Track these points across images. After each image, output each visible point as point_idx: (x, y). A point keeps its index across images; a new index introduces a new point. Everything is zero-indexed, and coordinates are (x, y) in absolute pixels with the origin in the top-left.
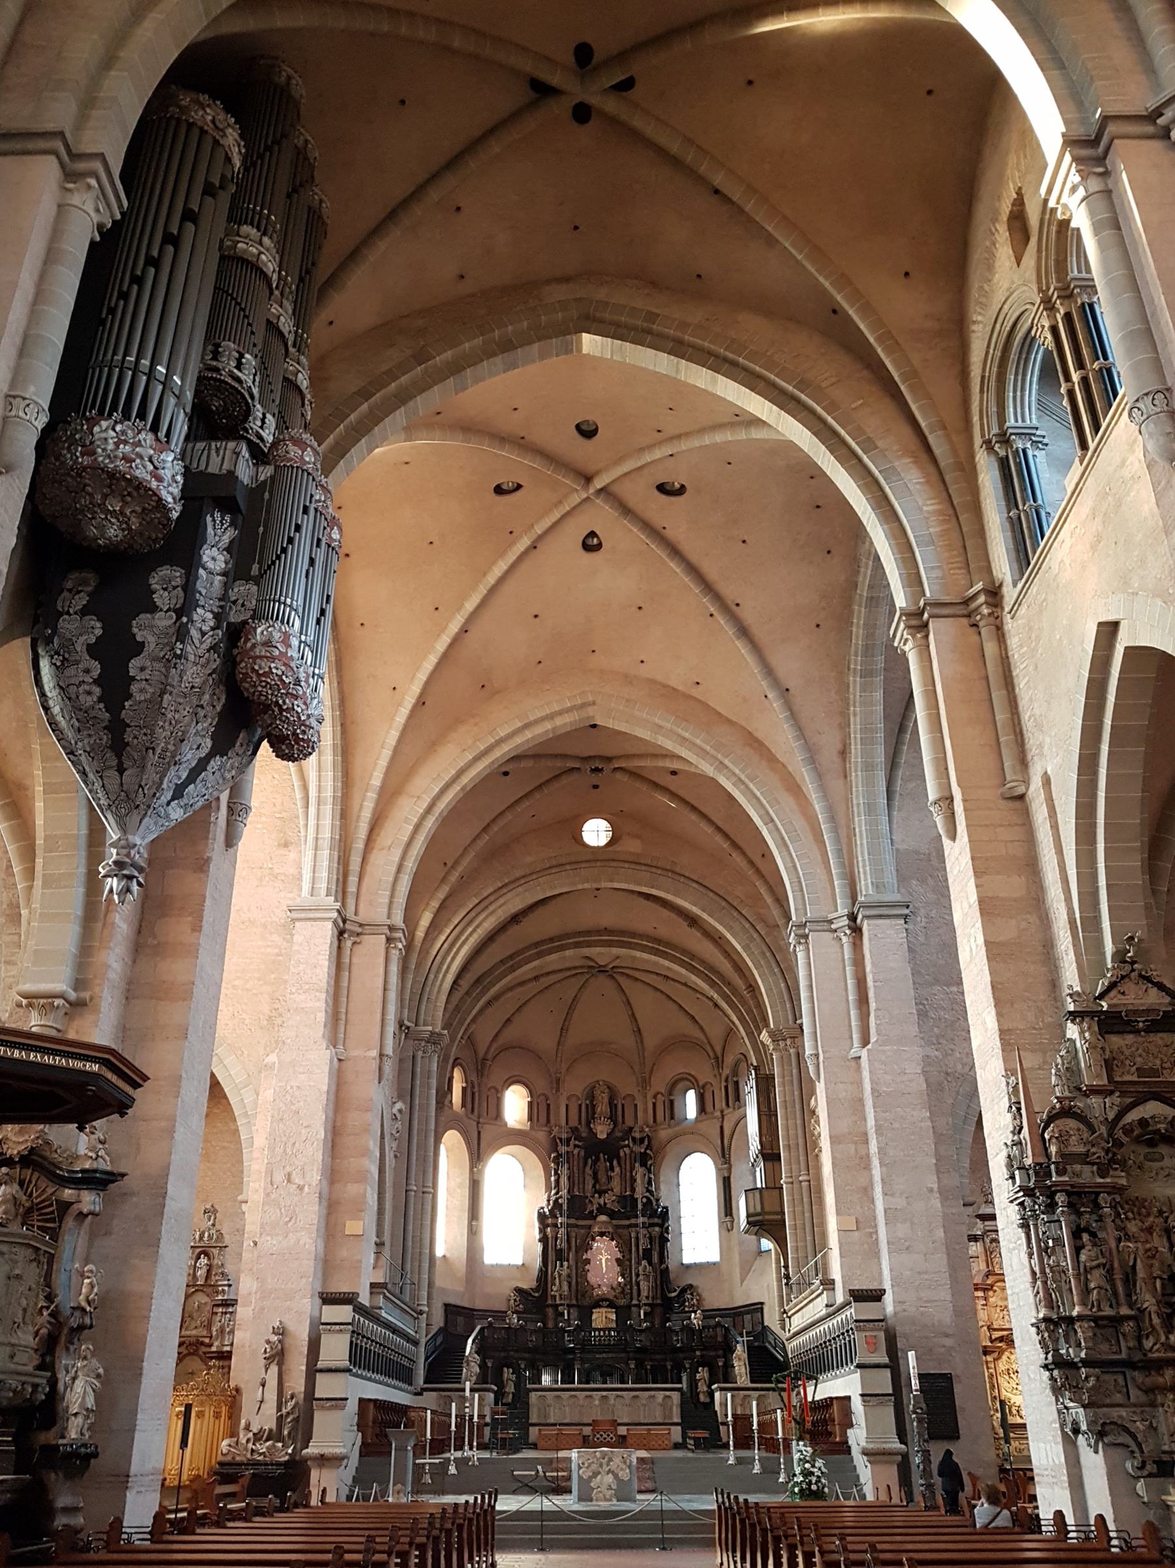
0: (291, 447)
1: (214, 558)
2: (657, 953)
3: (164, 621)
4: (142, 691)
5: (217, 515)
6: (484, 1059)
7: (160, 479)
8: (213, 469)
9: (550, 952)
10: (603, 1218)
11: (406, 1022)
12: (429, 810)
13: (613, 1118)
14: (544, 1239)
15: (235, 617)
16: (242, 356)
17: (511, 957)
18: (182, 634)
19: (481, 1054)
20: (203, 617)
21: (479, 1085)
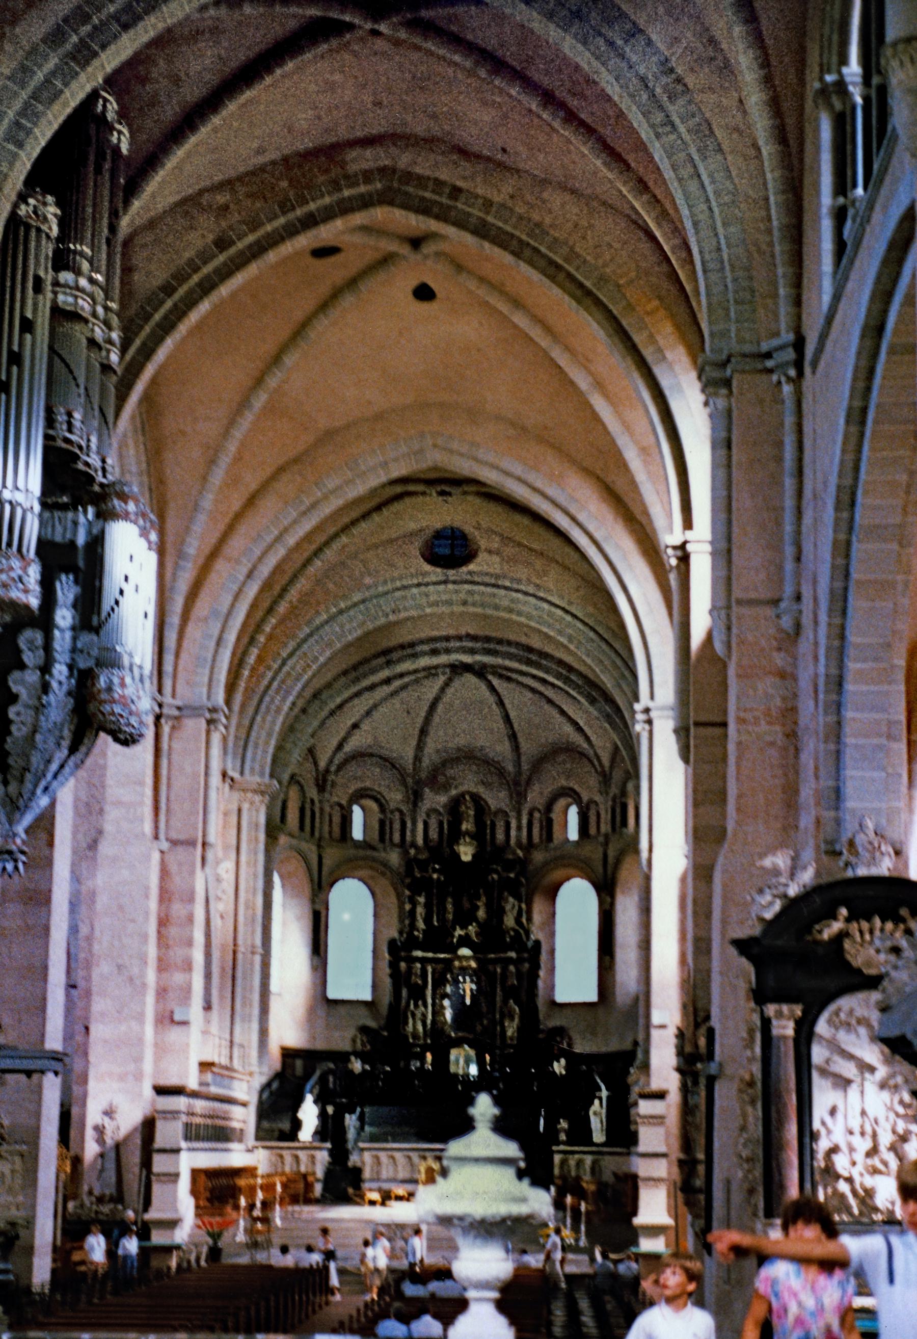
0: (116, 502)
1: (64, 617)
2: (529, 662)
3: (32, 677)
4: (19, 729)
5: (63, 577)
6: (327, 771)
7: (26, 591)
8: (58, 538)
9: (400, 660)
10: (465, 952)
11: (231, 773)
12: (250, 575)
13: (479, 836)
14: (395, 974)
15: (83, 664)
16: (69, 415)
17: (355, 668)
18: (45, 688)
19: (322, 764)
20: (60, 670)
21: (320, 802)
